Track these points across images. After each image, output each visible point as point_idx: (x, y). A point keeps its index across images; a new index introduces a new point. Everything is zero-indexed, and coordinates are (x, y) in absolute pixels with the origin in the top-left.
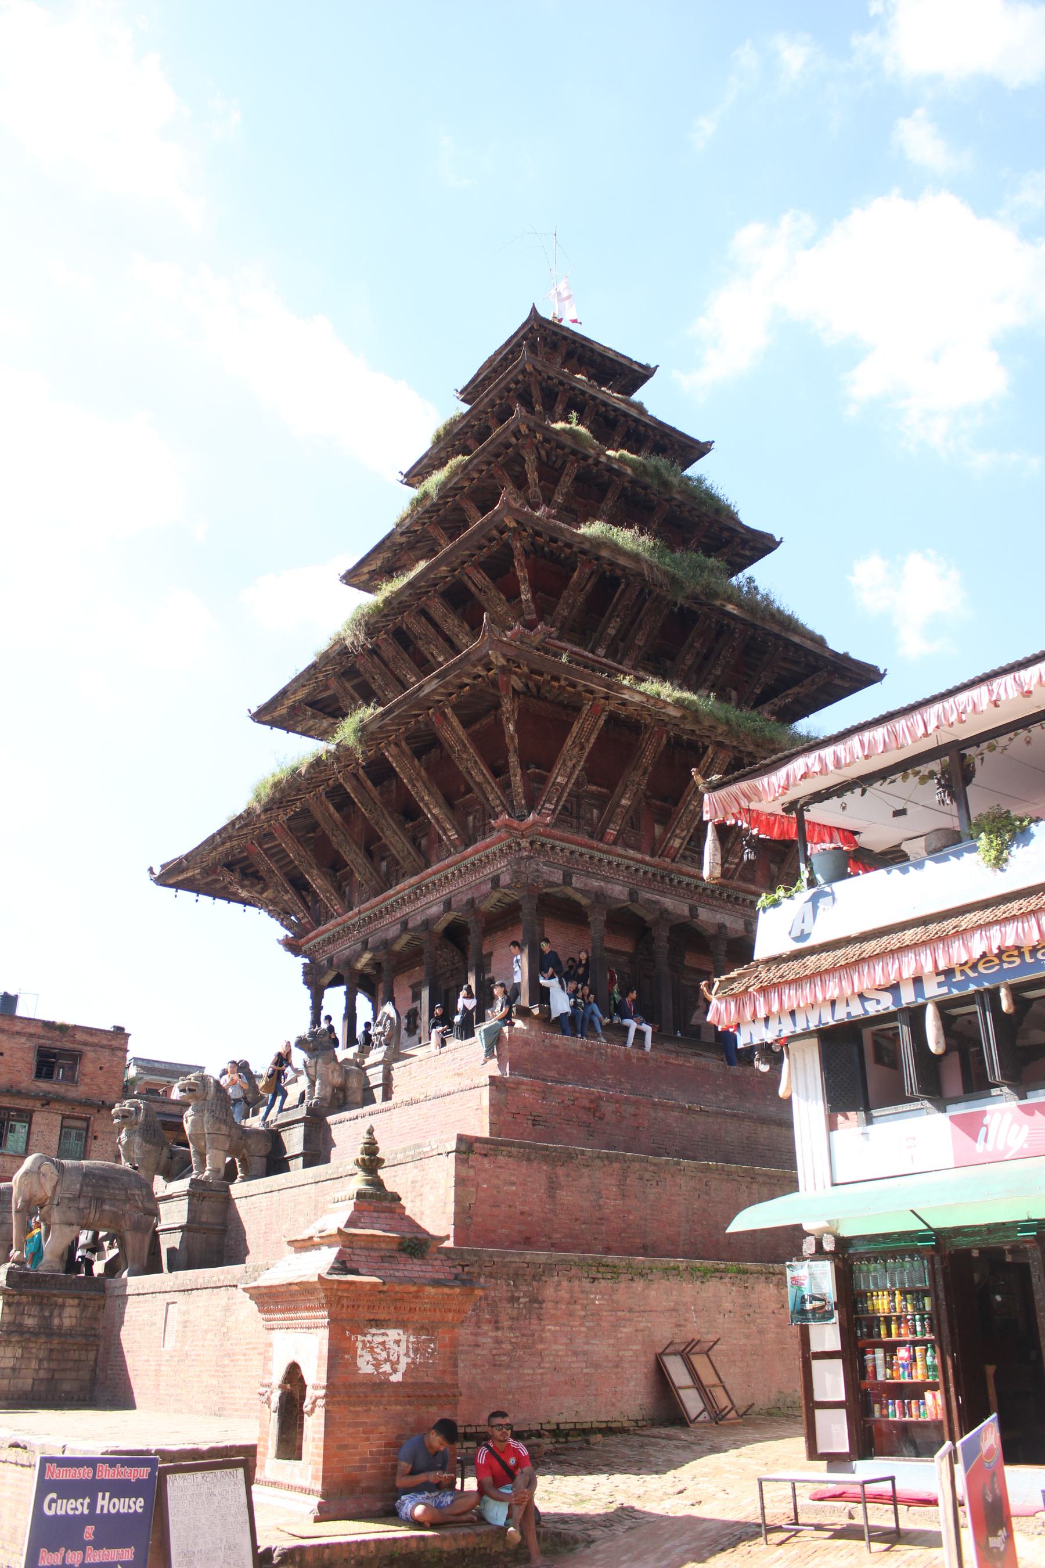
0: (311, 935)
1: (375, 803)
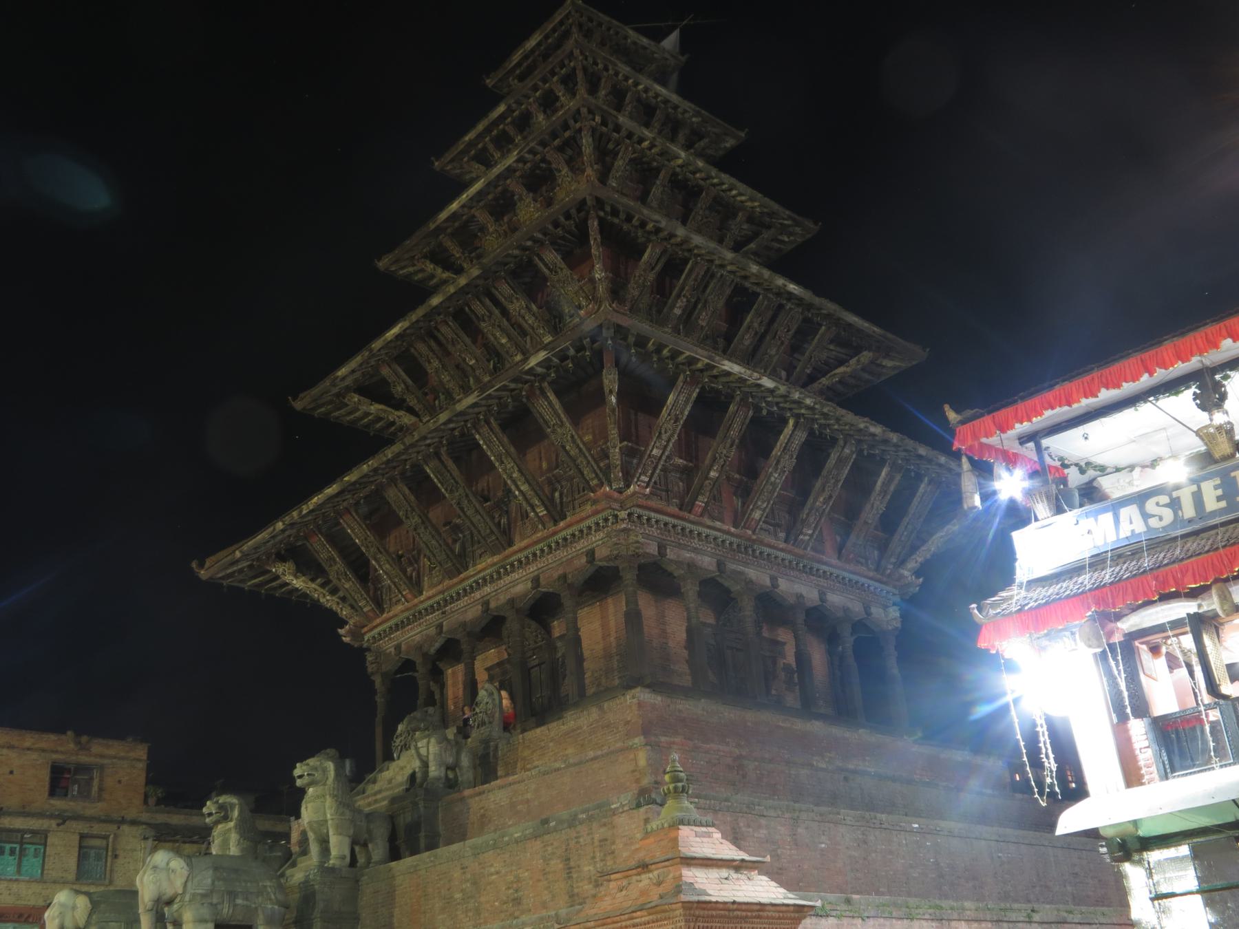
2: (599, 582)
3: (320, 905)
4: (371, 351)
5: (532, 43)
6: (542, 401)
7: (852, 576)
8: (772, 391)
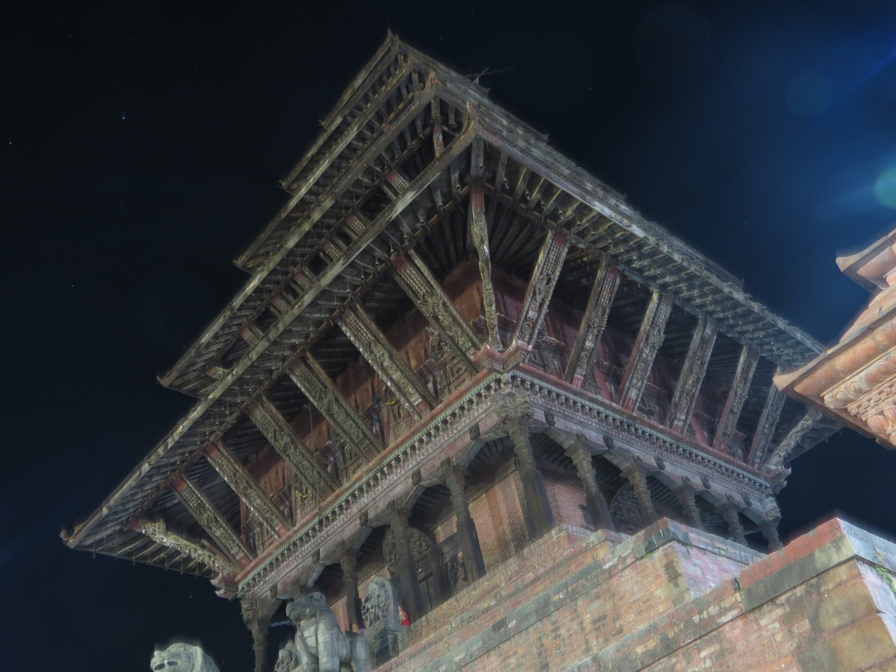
0: (248, 568)
1: (325, 387)
4: (232, 309)
5: (359, 82)
6: (410, 271)
7: (728, 466)
8: (641, 244)
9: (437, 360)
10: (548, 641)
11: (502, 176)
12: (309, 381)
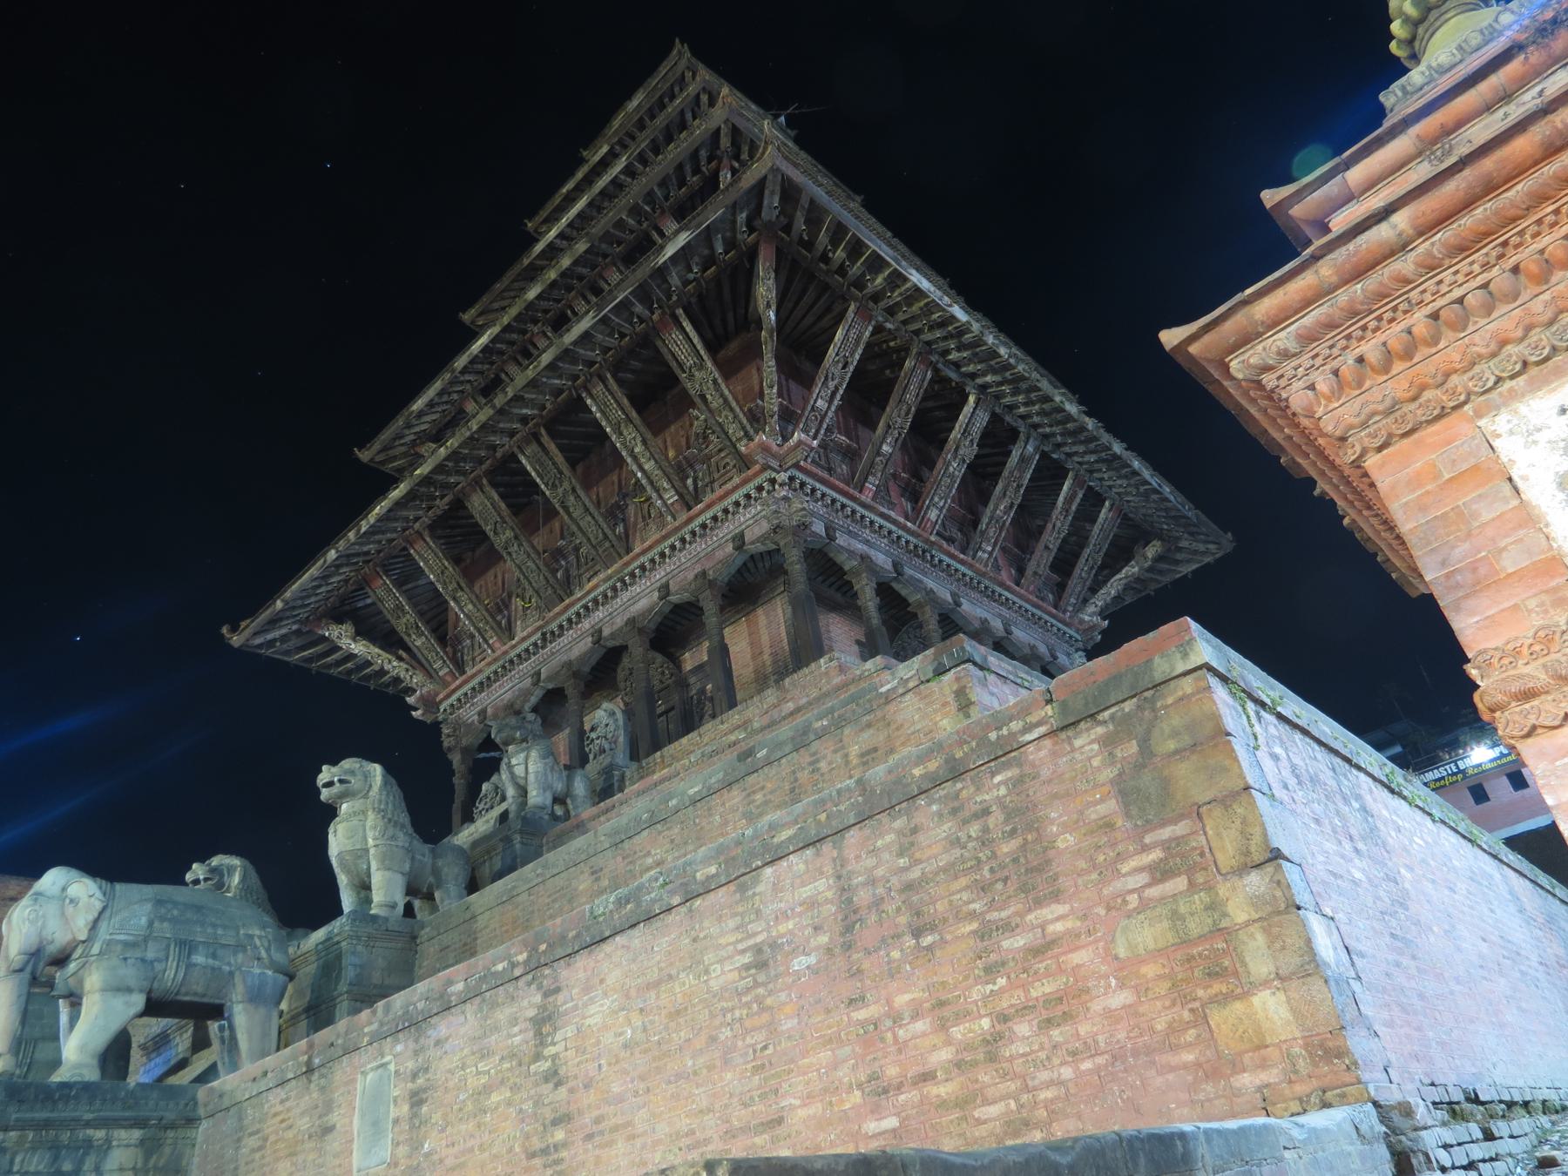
1: (561, 473)
2: (745, 586)
3: (349, 973)
4: (453, 371)
6: (676, 335)
8: (962, 330)
9: (700, 450)
10: (804, 776)
11: (800, 225)
12: (541, 464)
